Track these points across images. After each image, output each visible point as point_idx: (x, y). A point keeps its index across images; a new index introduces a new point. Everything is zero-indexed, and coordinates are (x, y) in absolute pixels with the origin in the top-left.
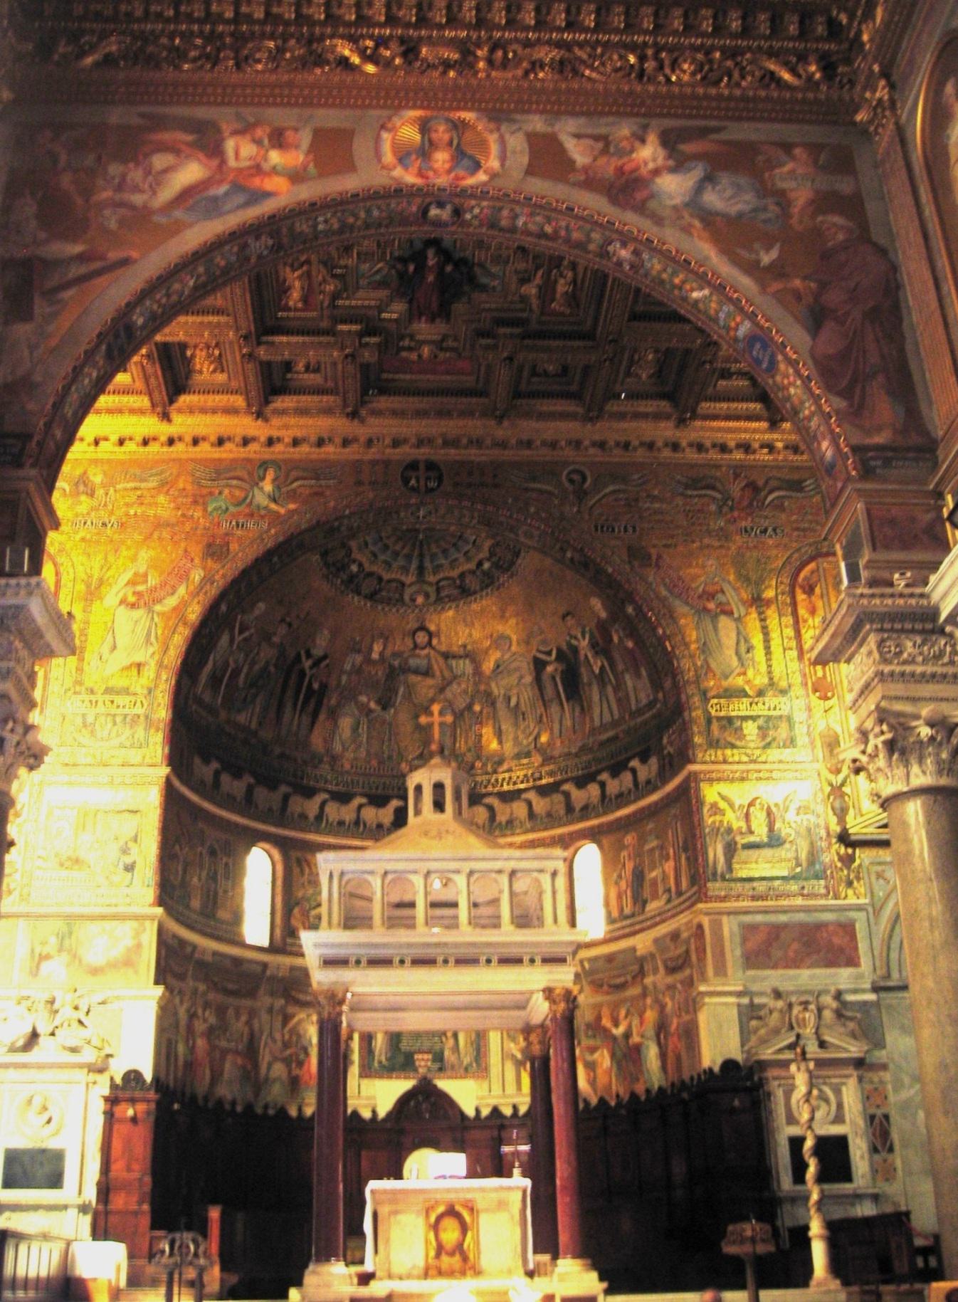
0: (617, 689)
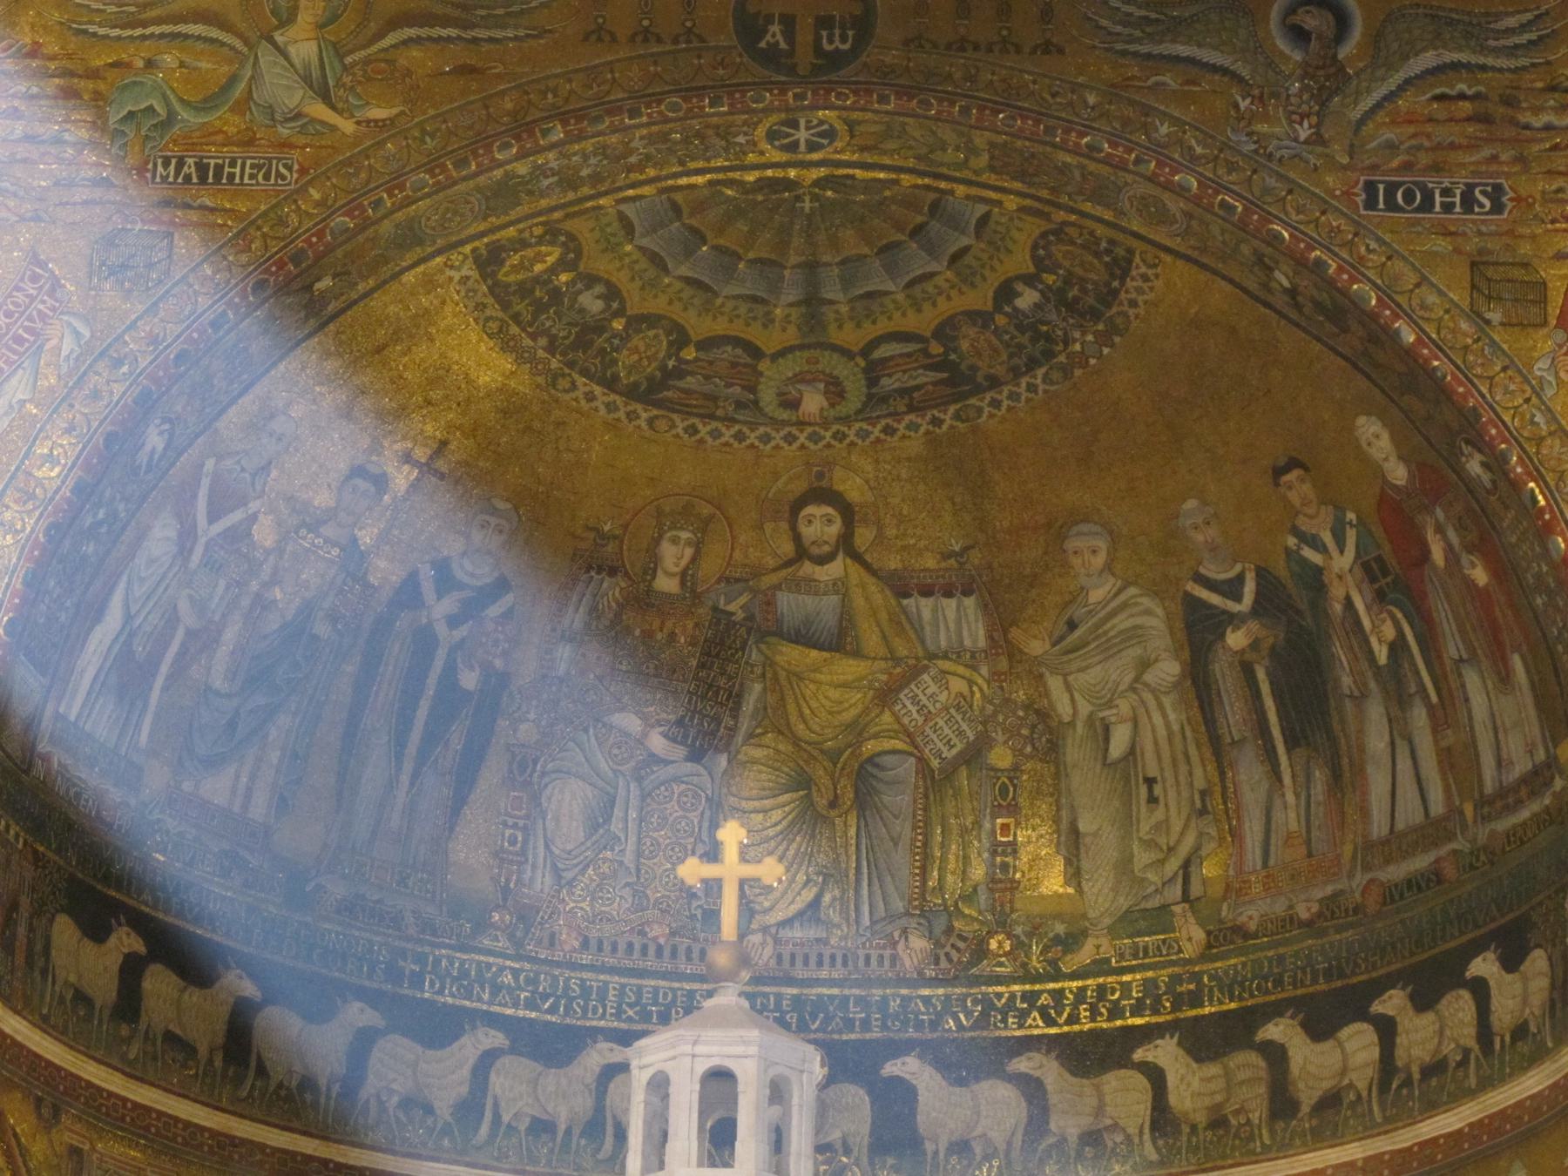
0: (1441, 718)
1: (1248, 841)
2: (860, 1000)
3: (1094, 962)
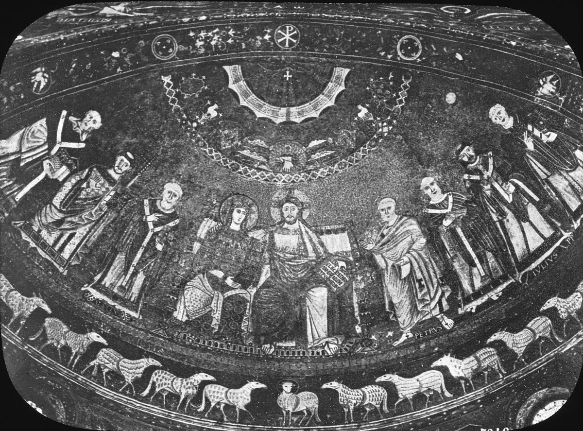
3: (405, 341)
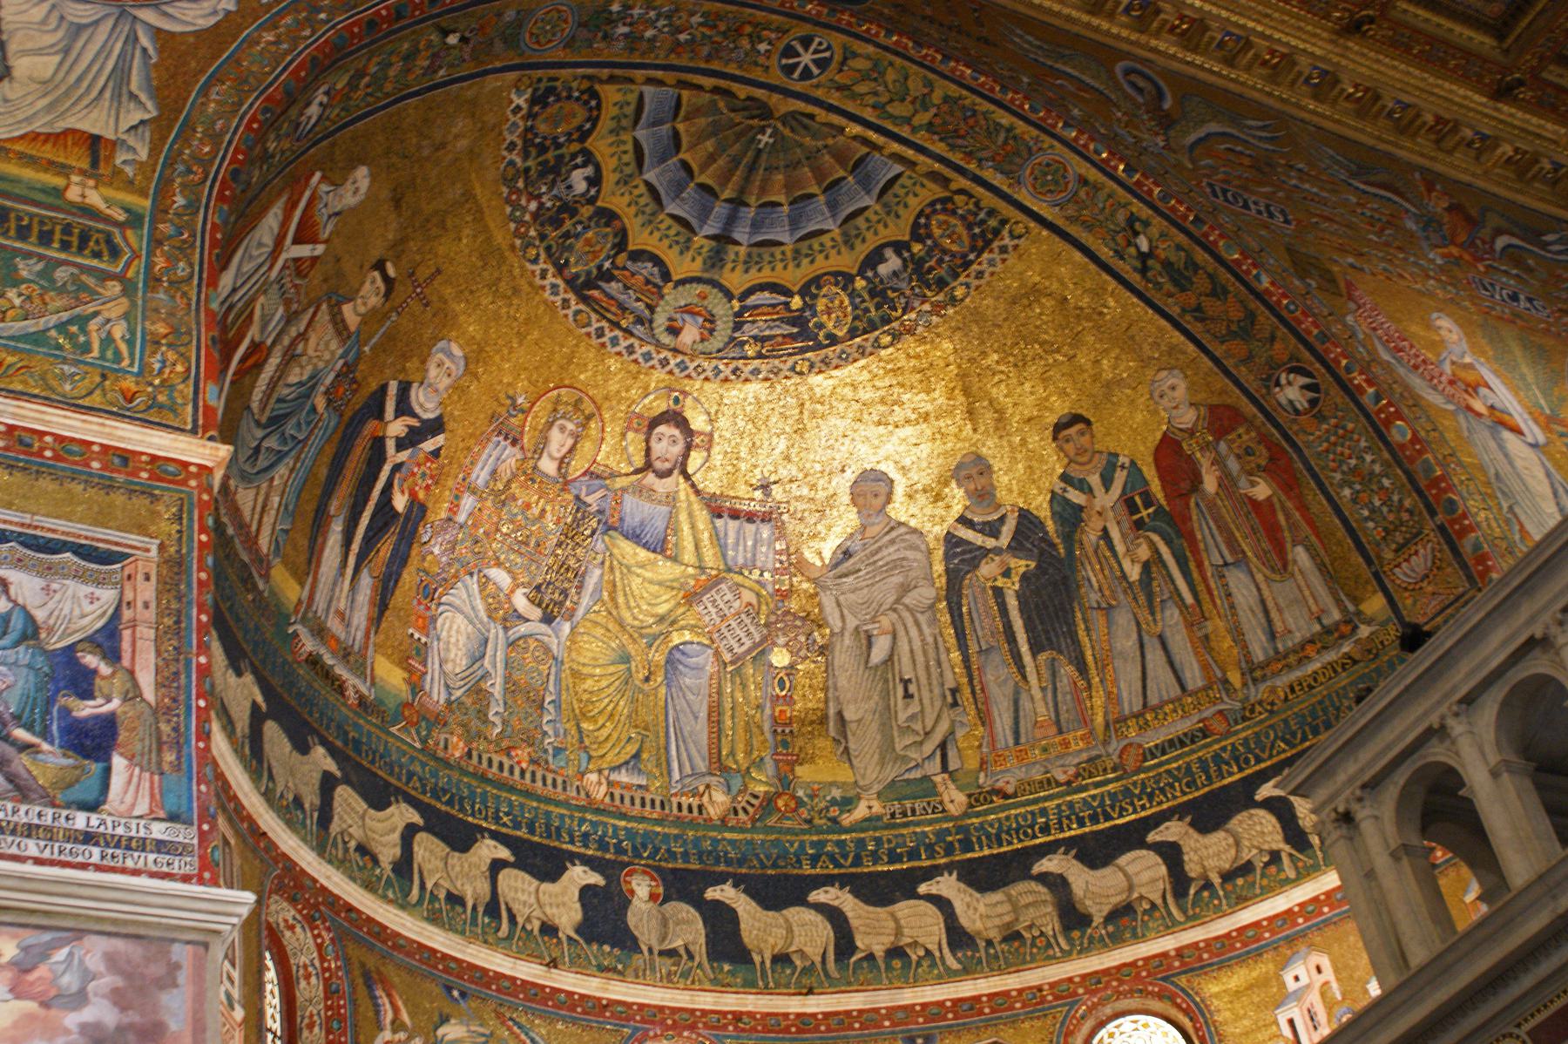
0: (1195, 618)
1: (998, 724)
2: (677, 837)
